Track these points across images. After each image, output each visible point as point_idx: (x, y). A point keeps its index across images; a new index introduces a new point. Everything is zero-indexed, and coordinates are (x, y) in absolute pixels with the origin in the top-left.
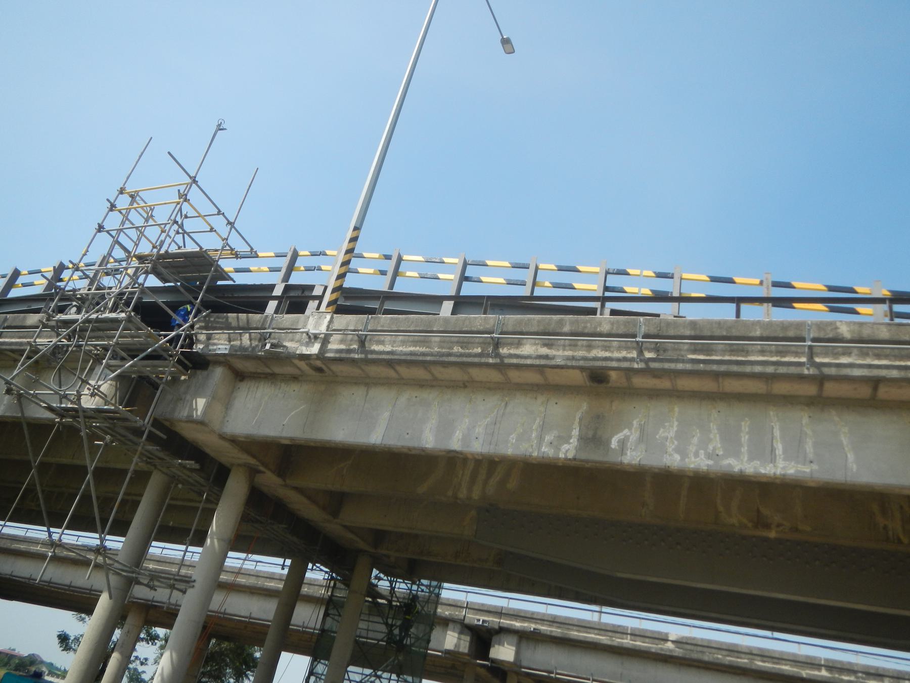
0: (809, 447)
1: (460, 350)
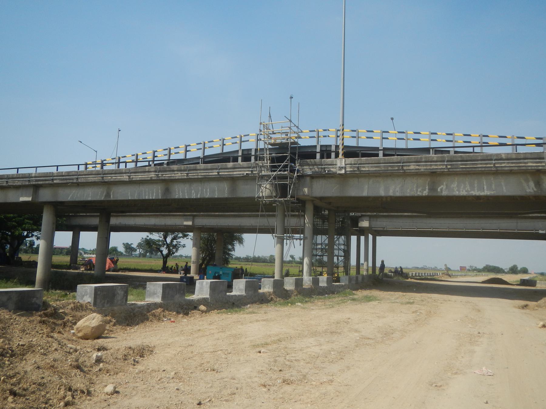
0: (493, 187)
1: (391, 169)
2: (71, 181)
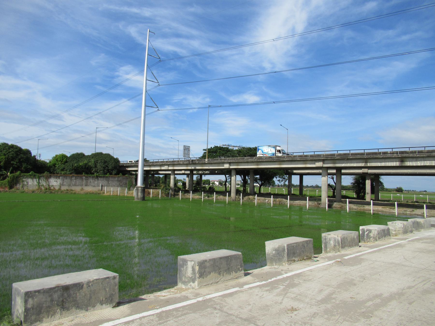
2: (347, 158)
